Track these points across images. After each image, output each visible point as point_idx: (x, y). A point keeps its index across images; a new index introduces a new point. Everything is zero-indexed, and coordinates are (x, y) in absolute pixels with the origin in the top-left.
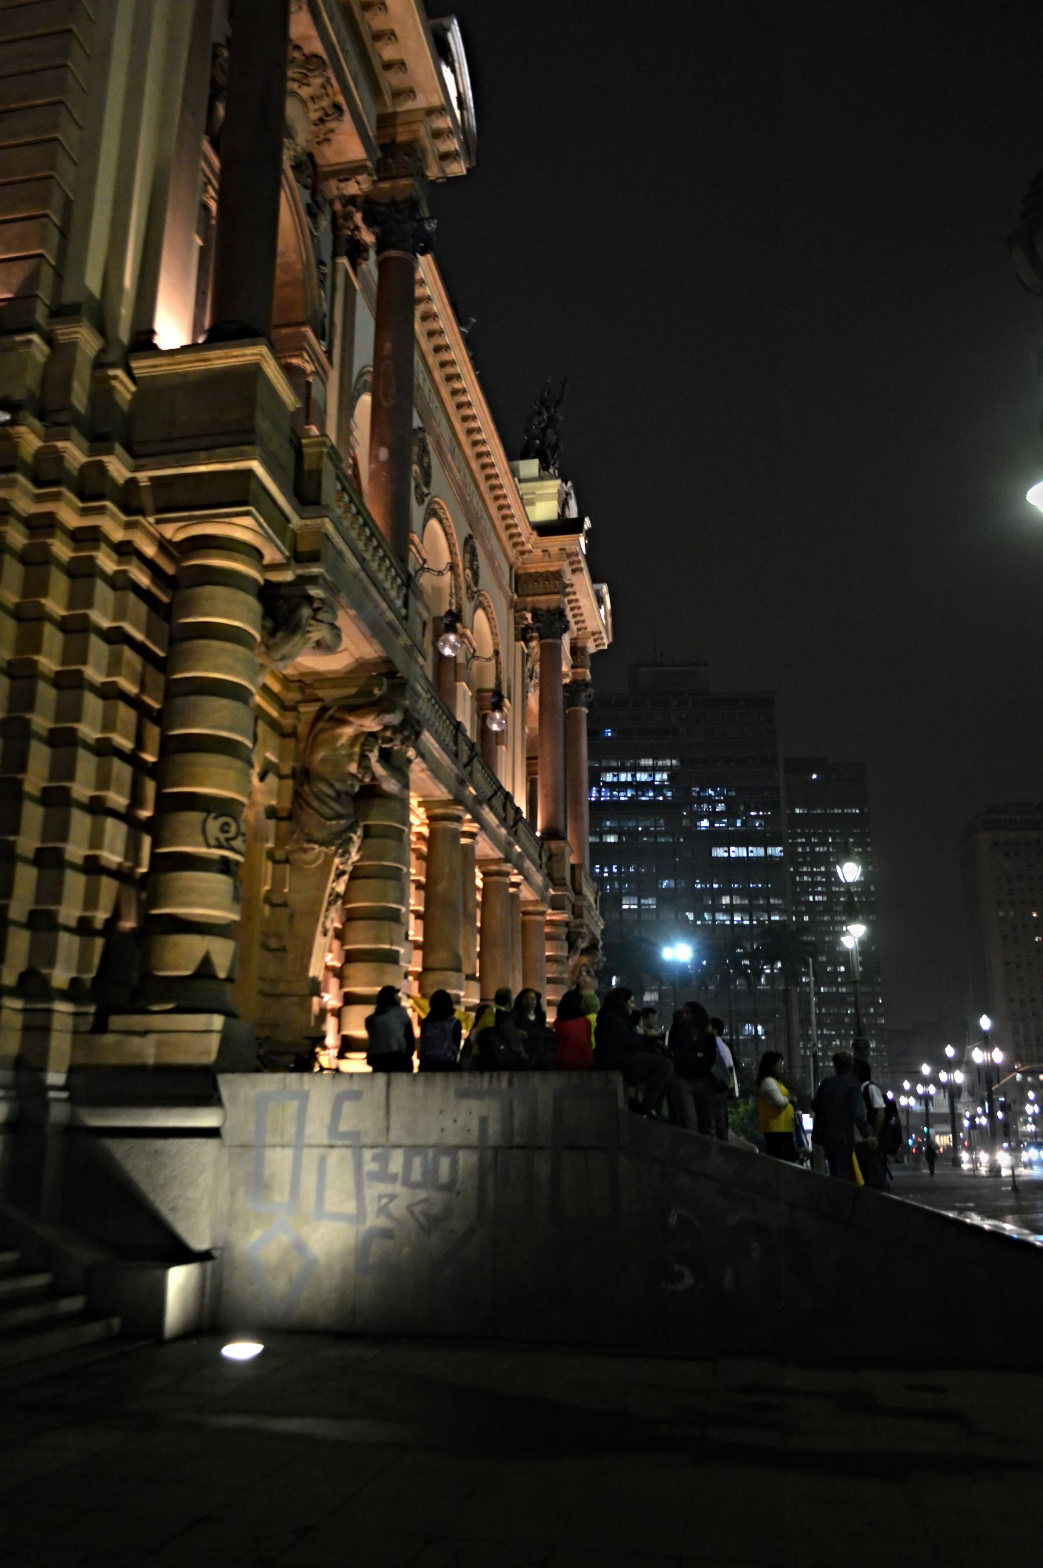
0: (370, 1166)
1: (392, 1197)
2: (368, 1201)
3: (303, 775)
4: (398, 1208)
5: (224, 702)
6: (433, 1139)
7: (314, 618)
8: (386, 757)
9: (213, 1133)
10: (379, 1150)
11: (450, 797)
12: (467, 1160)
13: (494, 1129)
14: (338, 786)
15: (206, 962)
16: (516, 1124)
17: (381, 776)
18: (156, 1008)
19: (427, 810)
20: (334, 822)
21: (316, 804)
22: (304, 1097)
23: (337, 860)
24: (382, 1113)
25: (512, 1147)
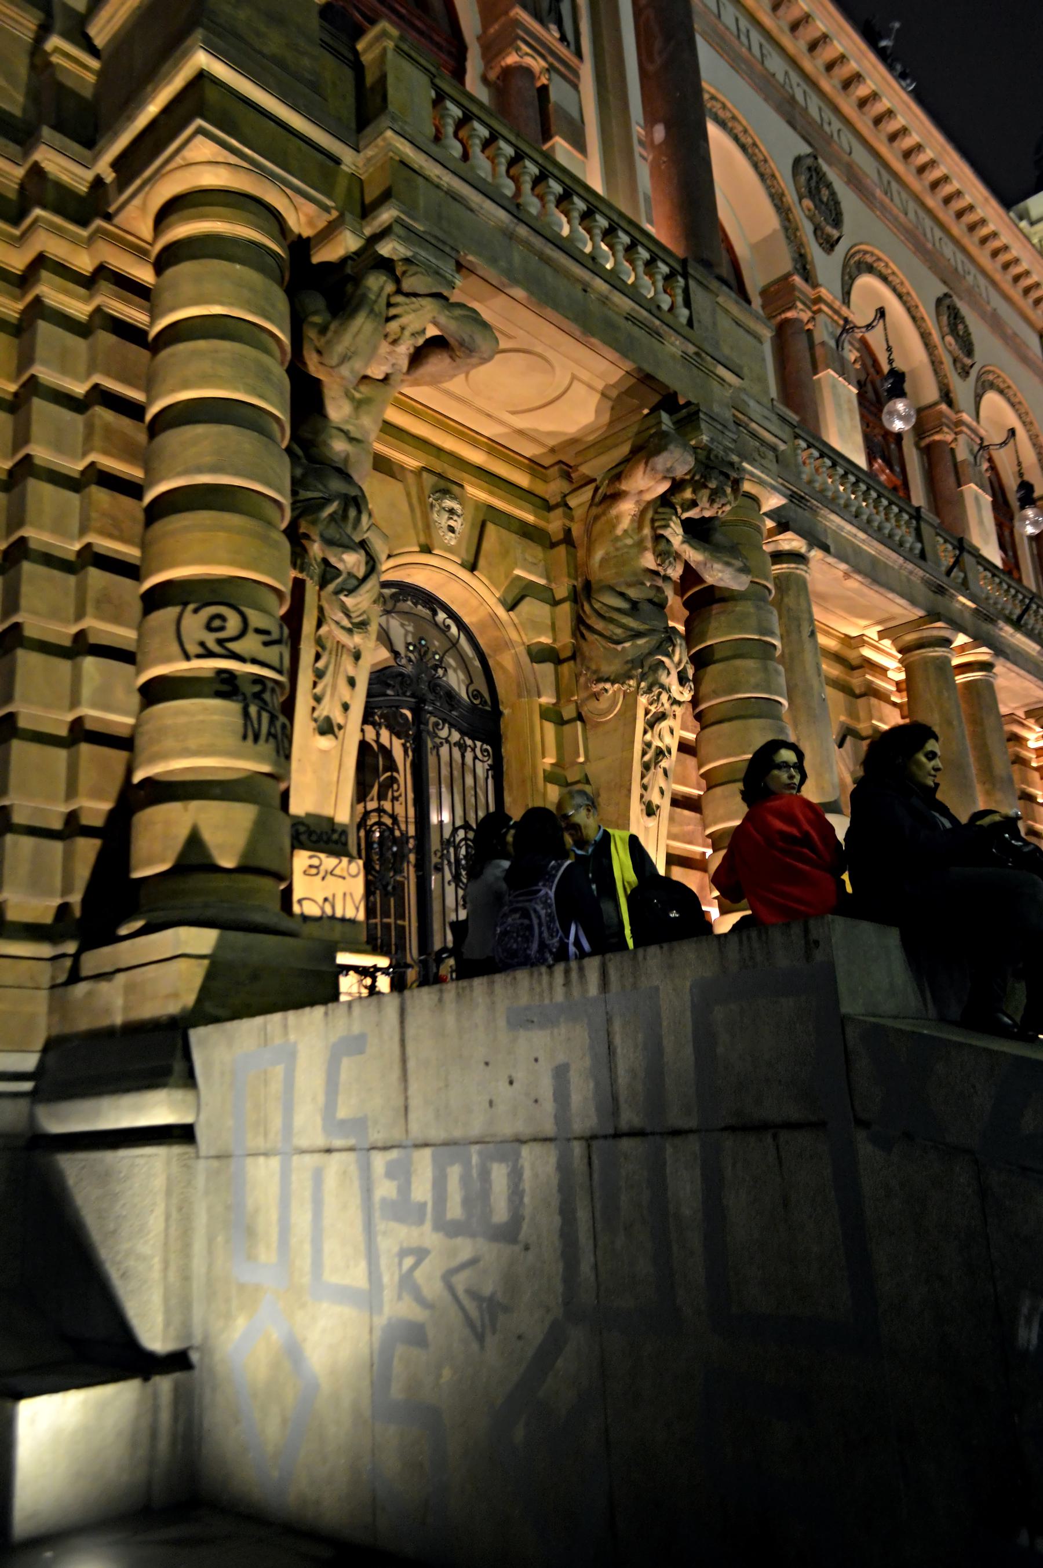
0: (385, 1189)
1: (421, 1254)
2: (384, 1262)
3: (584, 592)
4: (429, 1277)
6: (476, 1128)
7: (399, 291)
8: (699, 532)
9: (181, 1135)
10: (394, 1154)
11: (921, 613)
12: (539, 1165)
13: (581, 1093)
14: (633, 593)
15: (194, 841)
16: (623, 1078)
17: (698, 563)
18: (123, 931)
19: (894, 641)
20: (627, 645)
21: (599, 625)
22: (290, 1056)
23: (643, 700)
24: (396, 1074)
25: (617, 1135)
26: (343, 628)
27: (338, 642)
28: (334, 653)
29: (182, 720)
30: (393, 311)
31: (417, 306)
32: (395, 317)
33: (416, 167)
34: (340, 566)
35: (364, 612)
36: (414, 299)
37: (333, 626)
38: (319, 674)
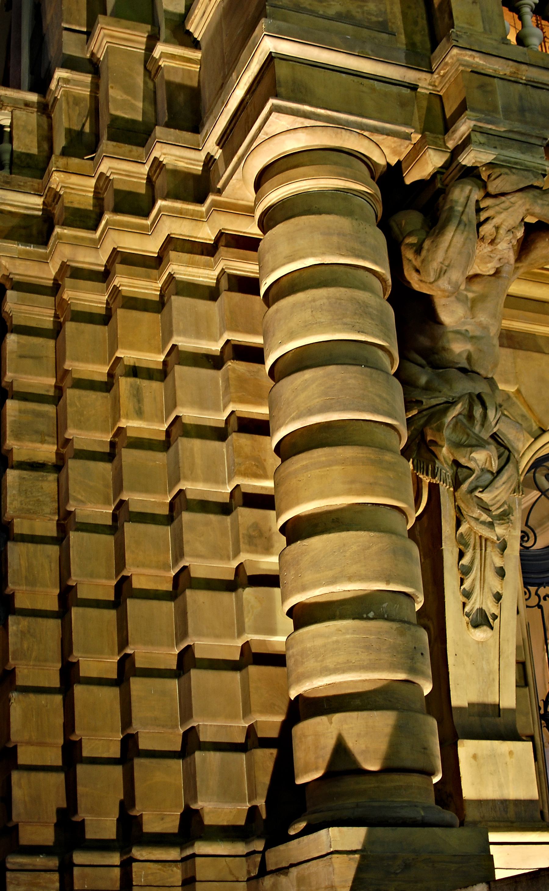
5: (308, 374)
7: (488, 195)
15: (341, 749)
18: (292, 832)
26: (483, 523)
27: (481, 537)
28: (478, 548)
29: (319, 642)
30: (483, 216)
31: (507, 204)
32: (487, 219)
33: (490, 72)
34: (472, 465)
35: (505, 503)
36: (503, 198)
37: (473, 523)
38: (465, 571)
